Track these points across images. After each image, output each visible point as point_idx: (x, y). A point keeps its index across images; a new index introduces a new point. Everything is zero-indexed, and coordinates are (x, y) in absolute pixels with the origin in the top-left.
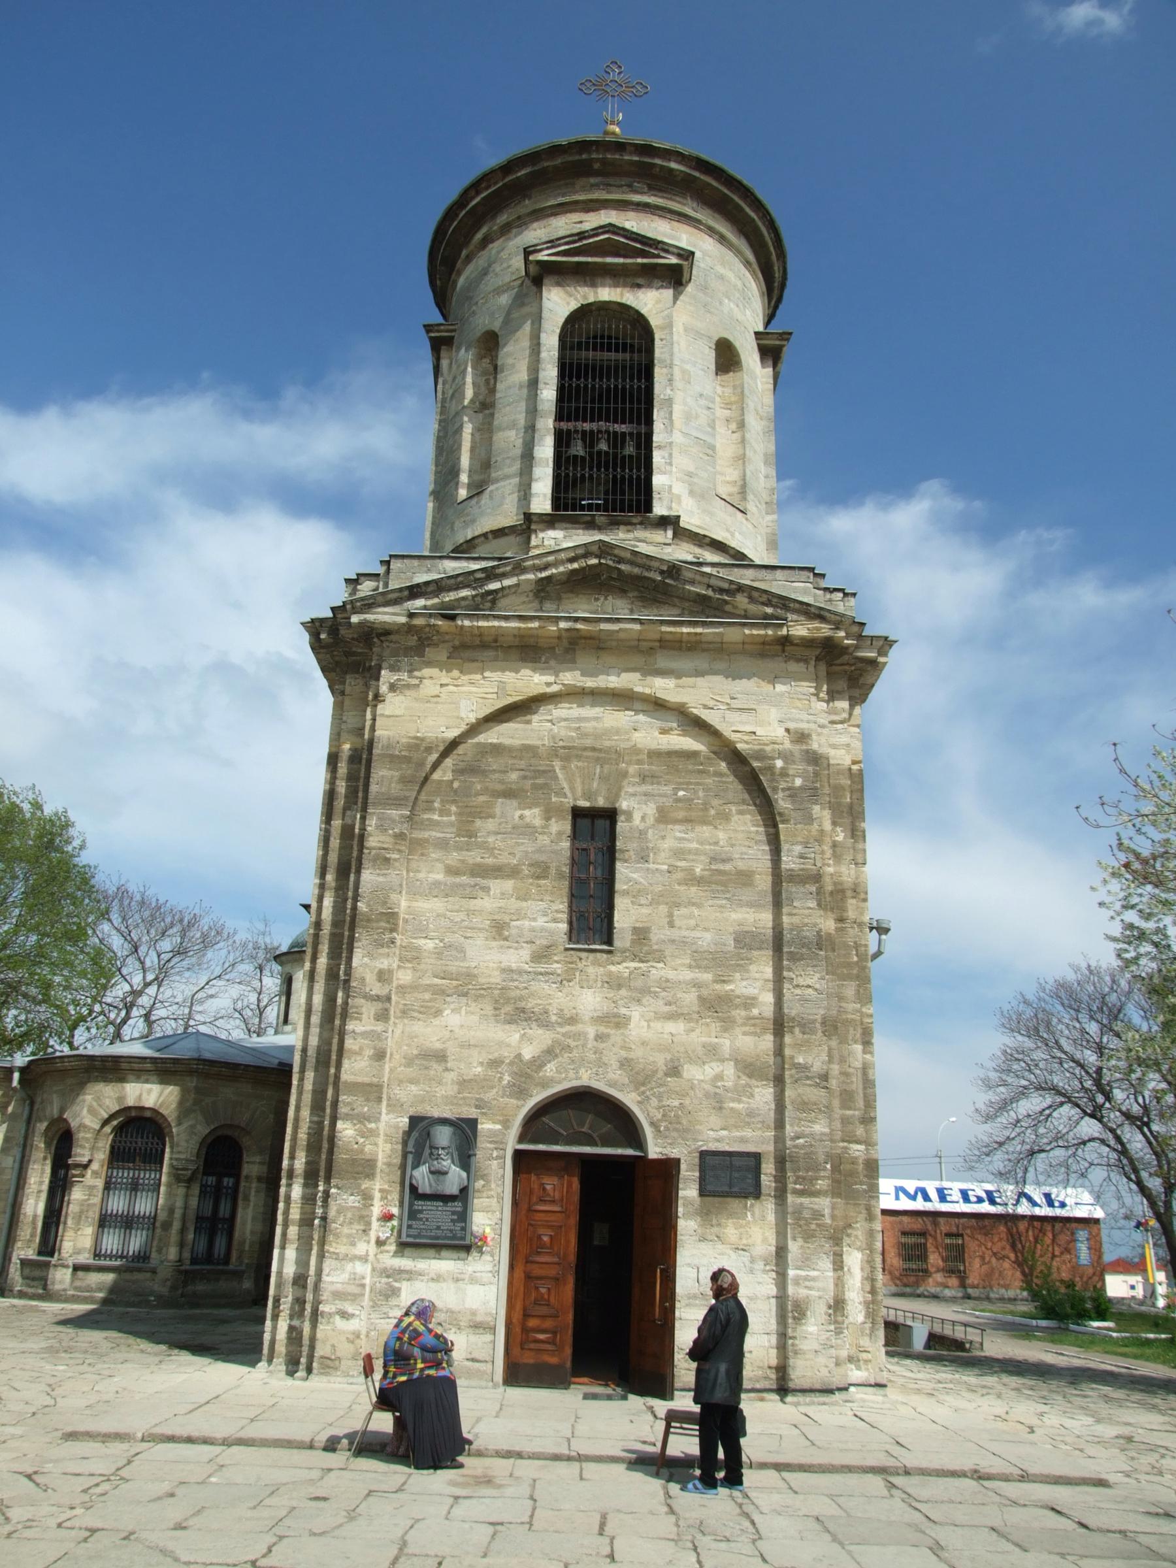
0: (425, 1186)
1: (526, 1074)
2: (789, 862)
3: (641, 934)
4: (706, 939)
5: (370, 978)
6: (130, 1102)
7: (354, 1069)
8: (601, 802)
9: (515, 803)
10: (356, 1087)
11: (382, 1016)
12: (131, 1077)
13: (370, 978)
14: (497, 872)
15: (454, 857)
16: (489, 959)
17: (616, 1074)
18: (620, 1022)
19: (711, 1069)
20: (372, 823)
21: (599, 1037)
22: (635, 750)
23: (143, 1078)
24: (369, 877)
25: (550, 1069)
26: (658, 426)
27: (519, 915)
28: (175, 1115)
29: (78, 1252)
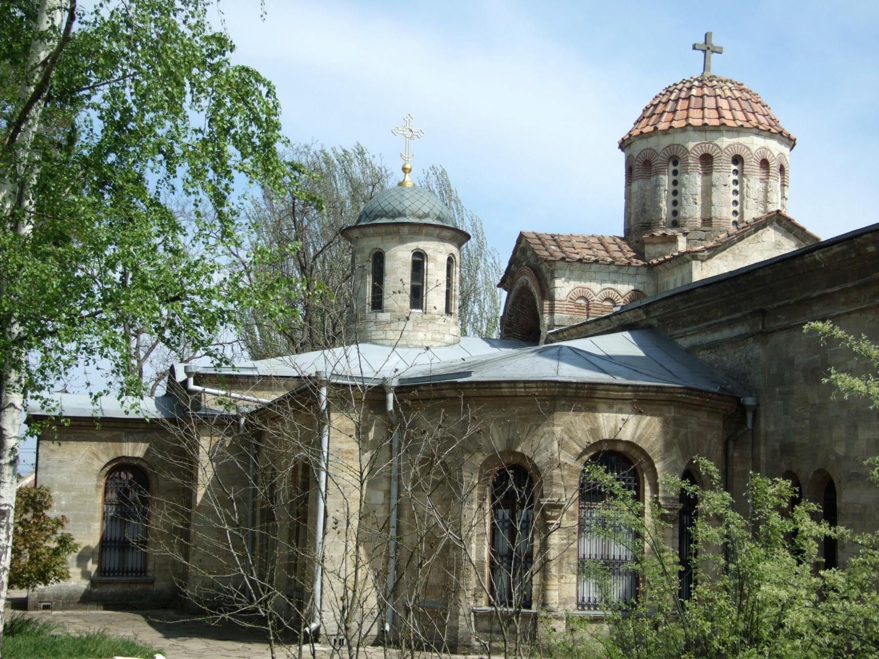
6: (606, 435)
12: (602, 406)
23: (615, 408)
28: (659, 447)
29: (563, 602)
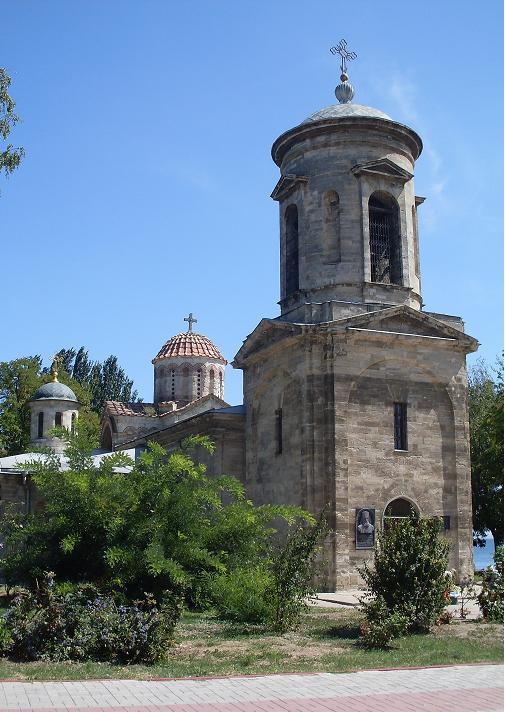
0: (363, 531)
1: (386, 493)
2: (456, 424)
3: (415, 446)
4: (432, 448)
5: (341, 462)
7: (340, 493)
8: (402, 400)
9: (376, 400)
10: (340, 500)
11: (346, 476)
13: (341, 462)
14: (373, 424)
15: (360, 419)
16: (373, 455)
17: (412, 493)
18: (411, 476)
19: (435, 491)
20: (336, 406)
21: (406, 481)
22: (411, 382)
24: (337, 426)
25: (393, 491)
26: (403, 248)
27: (381, 440)
